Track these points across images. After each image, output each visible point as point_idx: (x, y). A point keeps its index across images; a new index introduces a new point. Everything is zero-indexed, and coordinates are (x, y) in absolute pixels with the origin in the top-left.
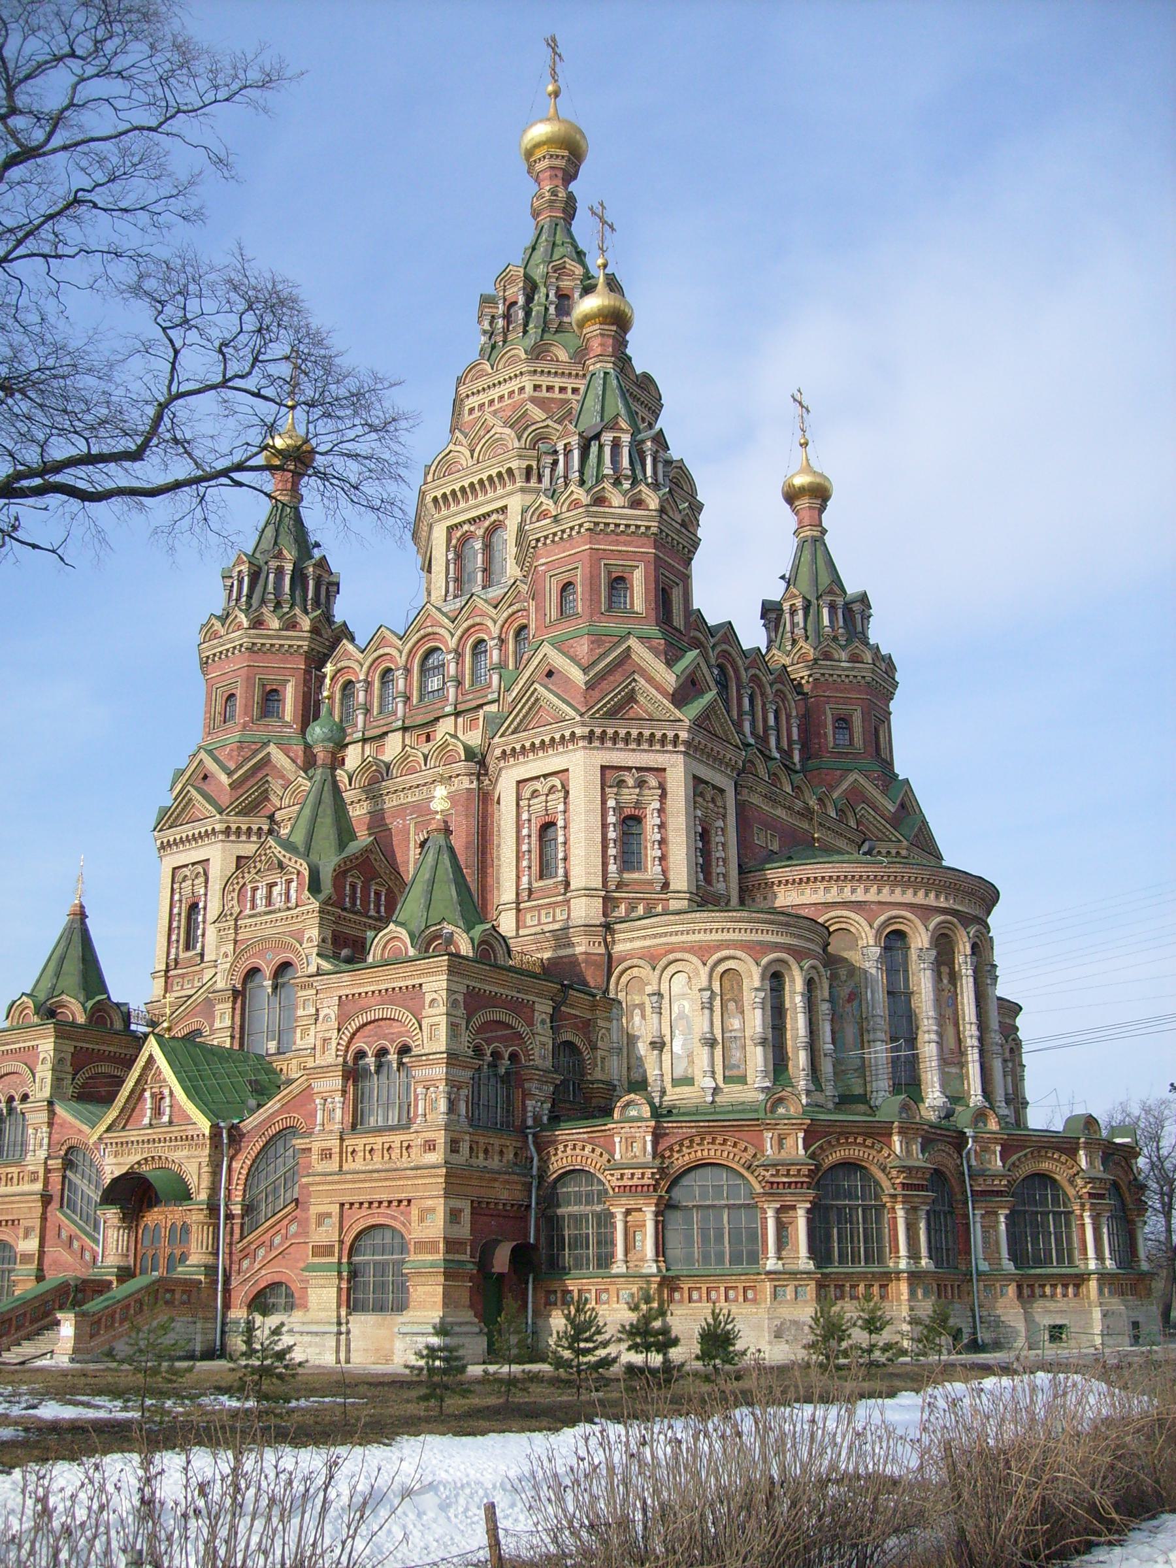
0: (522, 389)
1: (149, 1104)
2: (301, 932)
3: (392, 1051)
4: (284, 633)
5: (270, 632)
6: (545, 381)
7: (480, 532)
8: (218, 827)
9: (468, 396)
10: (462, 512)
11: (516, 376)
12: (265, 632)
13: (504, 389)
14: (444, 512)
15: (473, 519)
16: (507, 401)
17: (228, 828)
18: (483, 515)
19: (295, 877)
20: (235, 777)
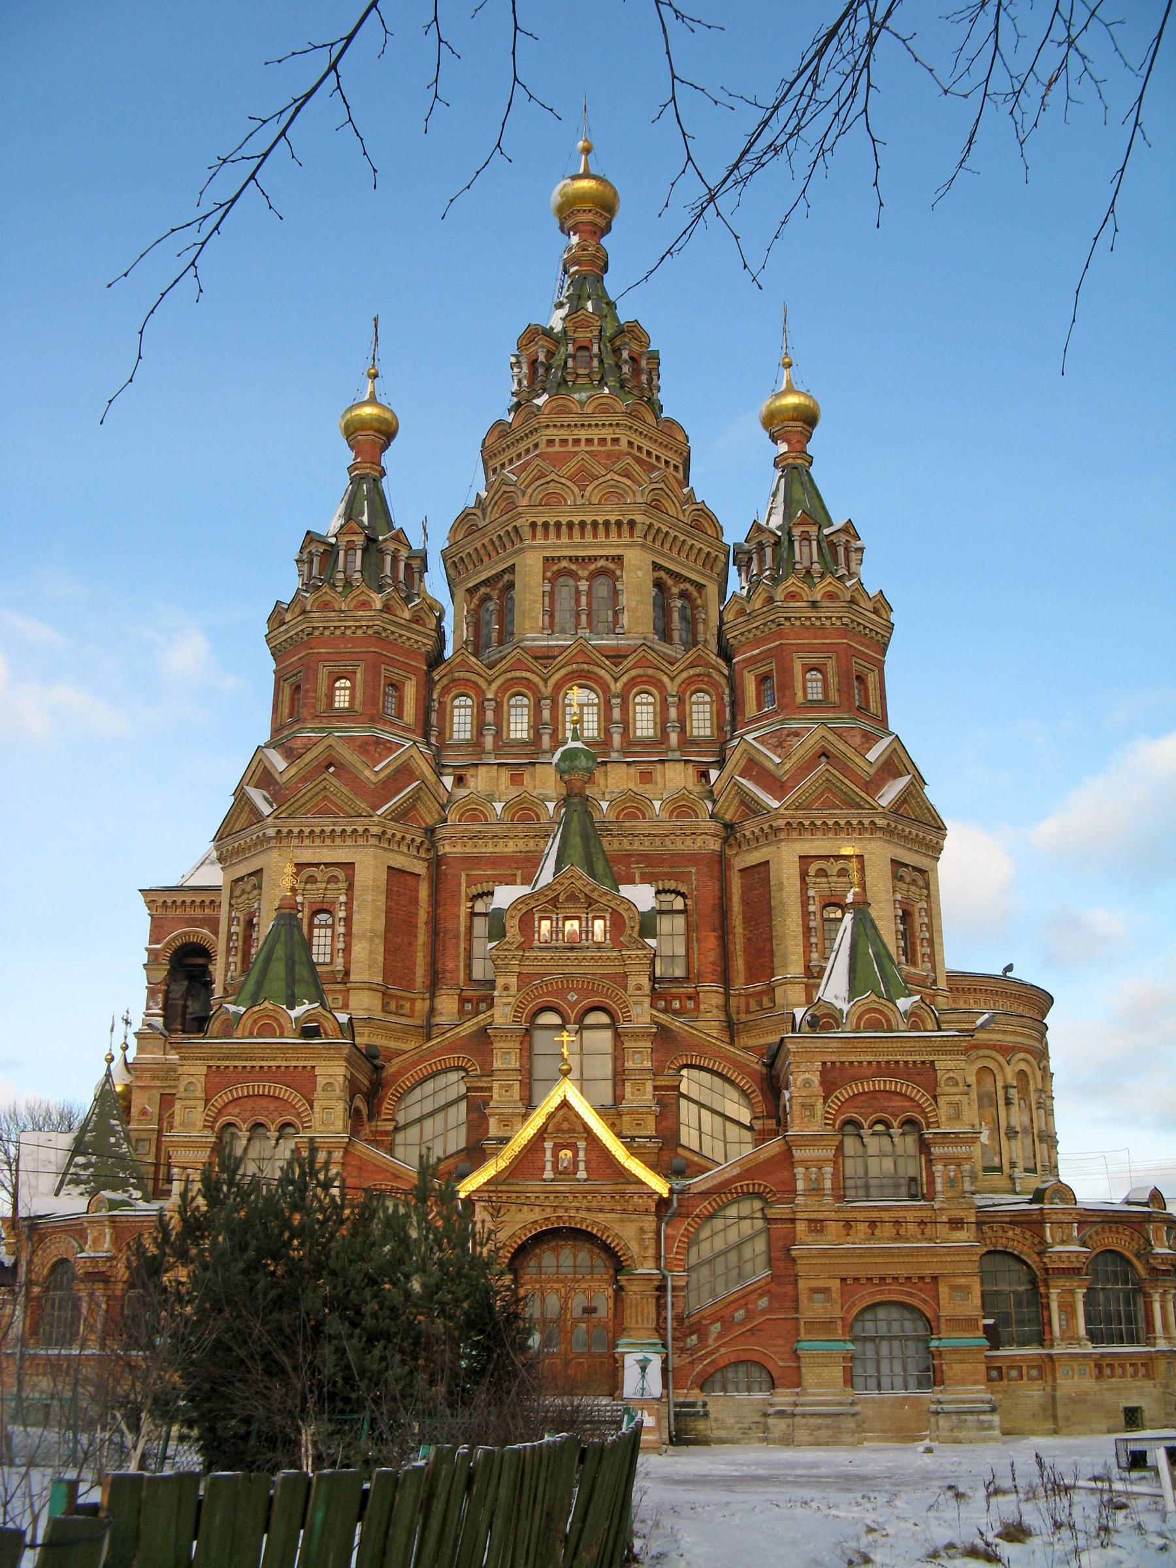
0: (615, 441)
1: (549, 1154)
2: (625, 976)
3: (895, 1124)
4: (414, 626)
5: (402, 622)
6: (638, 440)
7: (585, 574)
8: (375, 830)
9: (548, 426)
10: (565, 547)
11: (611, 425)
12: (394, 618)
13: (595, 434)
14: (540, 540)
15: (577, 558)
16: (583, 447)
17: (384, 833)
18: (590, 558)
19: (608, 916)
20: (382, 775)
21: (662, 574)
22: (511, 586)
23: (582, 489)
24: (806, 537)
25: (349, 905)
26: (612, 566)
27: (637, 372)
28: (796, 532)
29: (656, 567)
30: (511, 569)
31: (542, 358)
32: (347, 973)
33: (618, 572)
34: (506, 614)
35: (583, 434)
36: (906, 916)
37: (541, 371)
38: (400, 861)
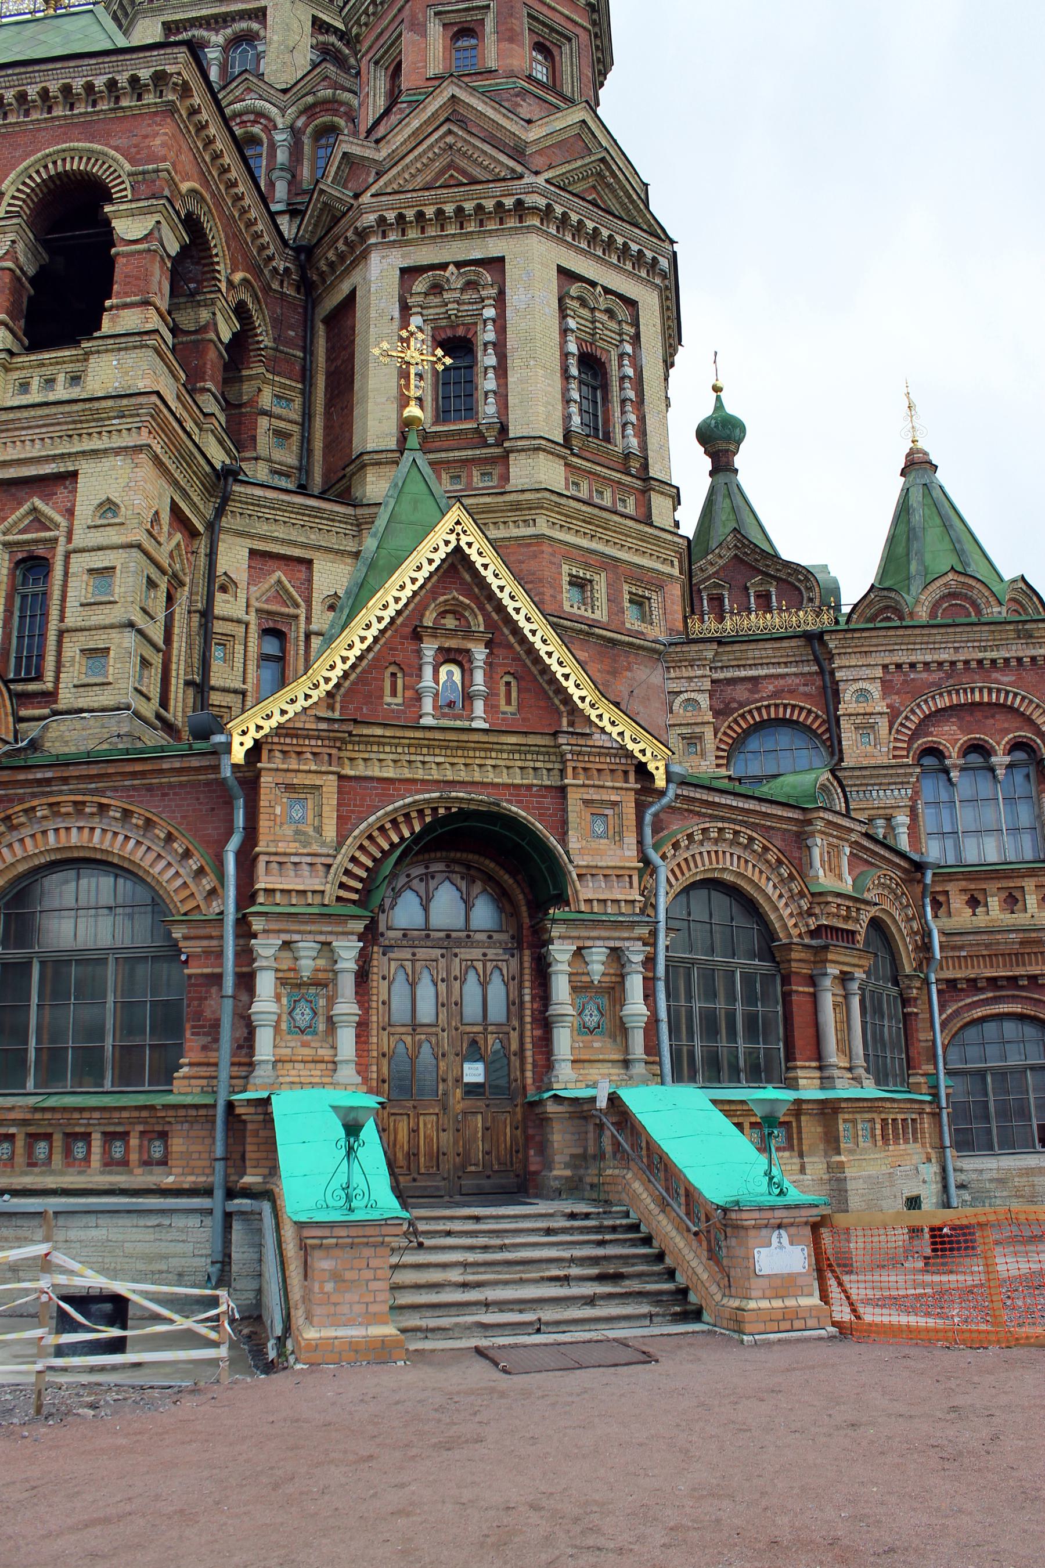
7: (217, 39)
21: (332, 39)
26: (255, 26)
33: (262, 33)
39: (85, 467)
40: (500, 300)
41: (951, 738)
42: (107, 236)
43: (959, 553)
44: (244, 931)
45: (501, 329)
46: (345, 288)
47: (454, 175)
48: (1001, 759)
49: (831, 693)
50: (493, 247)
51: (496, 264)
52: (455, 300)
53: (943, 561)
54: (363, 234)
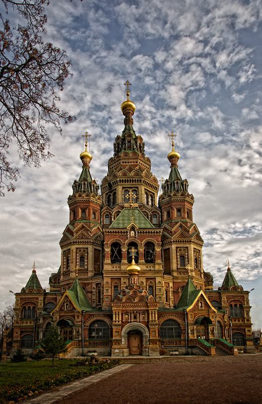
6: (141, 162)
22: (115, 193)
23: (130, 172)
24: (177, 183)
25: (87, 256)
27: (140, 147)
28: (175, 182)
29: (145, 189)
30: (116, 189)
31: (120, 143)
32: (87, 269)
34: (115, 198)
35: (130, 161)
36: (196, 259)
37: (120, 146)
38: (97, 248)
39: (156, 278)
40: (188, 252)
41: (233, 303)
42: (153, 250)
43: (234, 282)
44: (188, 326)
45: (188, 256)
46: (168, 247)
47: (182, 235)
48: (238, 306)
49: (220, 298)
50: (187, 246)
51: (187, 247)
52: (183, 252)
53: (232, 283)
54: (171, 242)
